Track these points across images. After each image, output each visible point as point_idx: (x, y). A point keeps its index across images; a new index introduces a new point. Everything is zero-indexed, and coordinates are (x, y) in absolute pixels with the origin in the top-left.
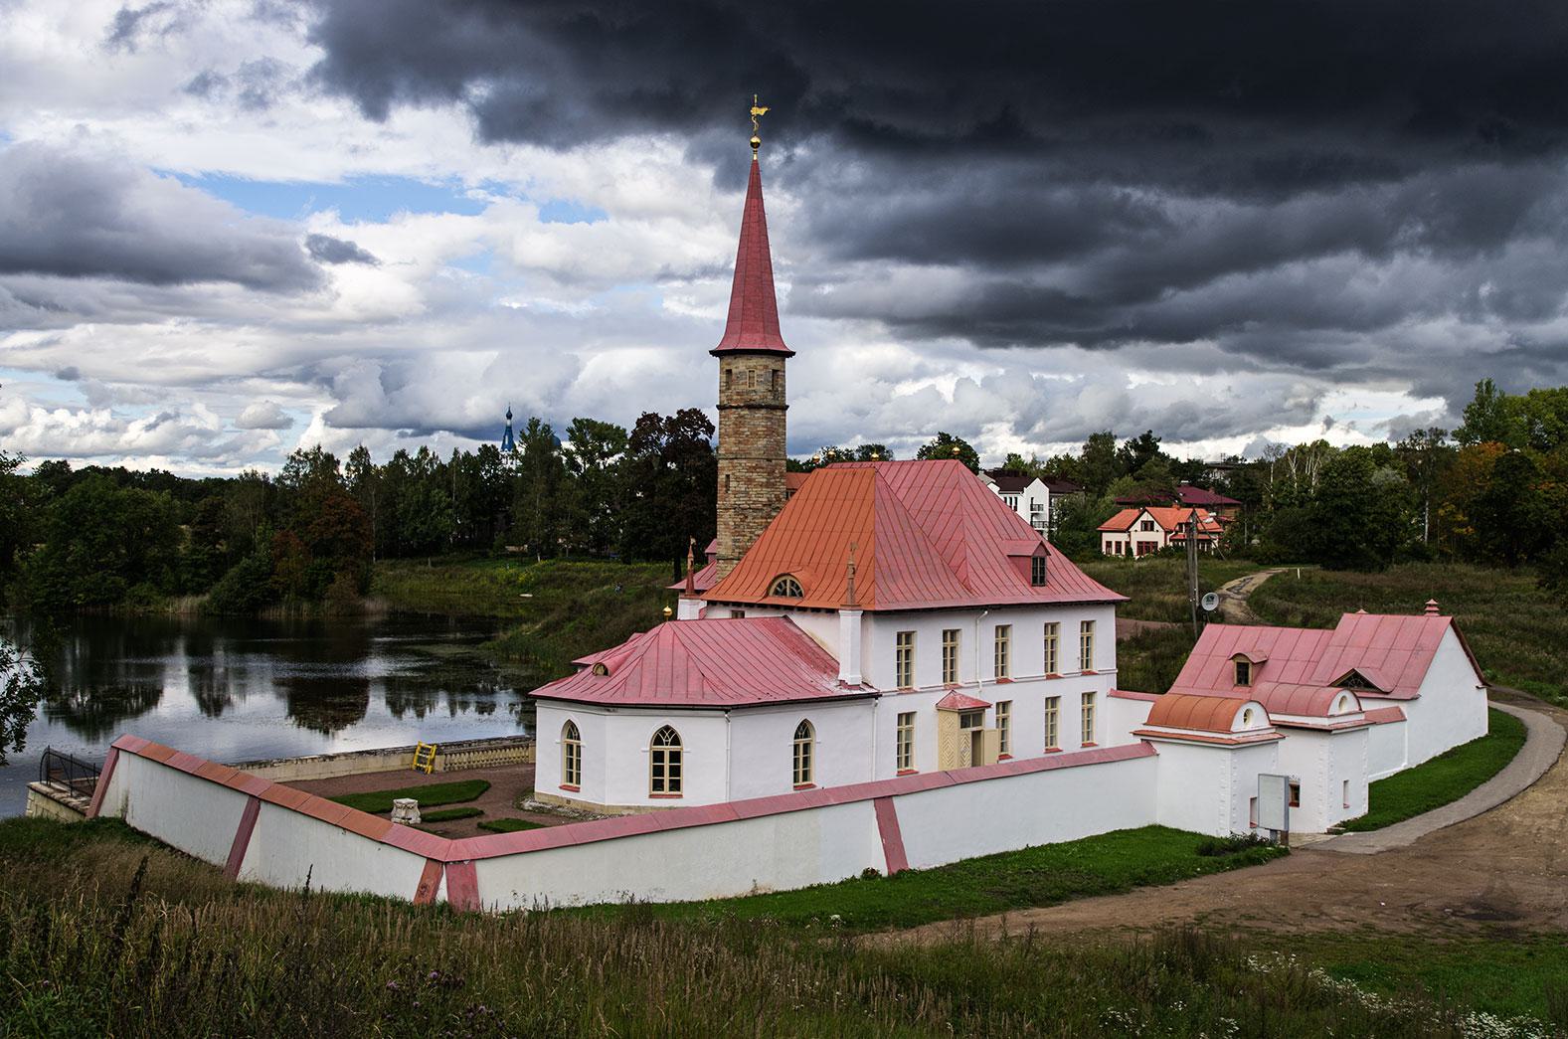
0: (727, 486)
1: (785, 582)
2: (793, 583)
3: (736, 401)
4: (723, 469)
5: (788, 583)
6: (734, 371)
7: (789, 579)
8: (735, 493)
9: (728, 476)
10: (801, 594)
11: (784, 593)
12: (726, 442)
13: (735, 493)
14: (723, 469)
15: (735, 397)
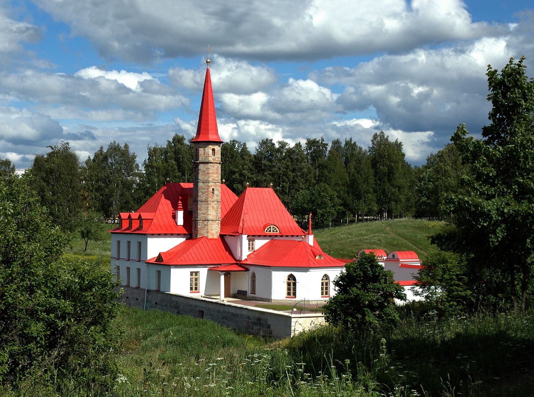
0: (213, 193)
1: (270, 228)
2: (273, 227)
3: (217, 161)
4: (211, 186)
5: (272, 228)
6: (216, 149)
7: (272, 226)
8: (216, 195)
9: (213, 189)
10: (277, 231)
11: (270, 231)
12: (213, 176)
13: (216, 195)
14: (211, 186)
15: (217, 159)
